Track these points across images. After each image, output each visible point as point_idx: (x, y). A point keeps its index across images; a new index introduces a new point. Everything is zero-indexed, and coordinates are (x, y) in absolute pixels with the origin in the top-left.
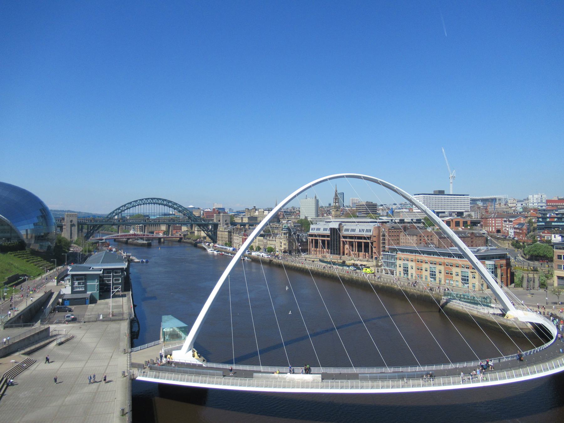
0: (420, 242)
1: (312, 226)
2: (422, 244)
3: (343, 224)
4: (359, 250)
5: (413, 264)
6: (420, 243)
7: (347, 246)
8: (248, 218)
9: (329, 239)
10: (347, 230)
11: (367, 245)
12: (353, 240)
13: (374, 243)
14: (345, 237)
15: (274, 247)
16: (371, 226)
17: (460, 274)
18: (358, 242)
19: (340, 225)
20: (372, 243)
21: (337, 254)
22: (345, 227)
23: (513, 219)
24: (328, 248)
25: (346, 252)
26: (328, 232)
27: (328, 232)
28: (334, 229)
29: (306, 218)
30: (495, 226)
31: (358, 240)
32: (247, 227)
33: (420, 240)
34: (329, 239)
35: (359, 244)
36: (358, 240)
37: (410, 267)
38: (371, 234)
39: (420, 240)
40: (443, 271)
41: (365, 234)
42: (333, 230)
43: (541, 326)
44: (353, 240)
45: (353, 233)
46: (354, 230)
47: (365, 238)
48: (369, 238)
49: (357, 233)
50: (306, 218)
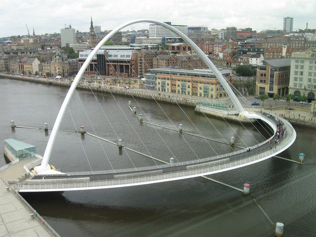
0: (168, 64)
1: (81, 53)
2: (170, 66)
3: (107, 51)
4: (122, 71)
5: (169, 82)
6: (169, 65)
7: (112, 68)
8: (16, 46)
9: (96, 63)
10: (110, 56)
11: (127, 67)
12: (116, 64)
13: (133, 66)
14: (108, 62)
15: (49, 72)
16: (130, 53)
17: (203, 88)
18: (120, 65)
19: (105, 51)
20: (131, 65)
21: (103, 75)
22: (109, 54)
23: (221, 46)
24: (96, 70)
25: (111, 73)
26: (96, 58)
27: (96, 58)
28: (100, 55)
29: (68, 45)
30: (209, 50)
31: (120, 64)
32: (19, 54)
33: (169, 63)
34: (96, 63)
35: (121, 67)
36: (120, 64)
37: (166, 84)
38: (130, 58)
39: (169, 63)
40: (191, 87)
41: (125, 58)
42: (99, 56)
43: (259, 120)
44: (116, 64)
45: (115, 58)
46: (116, 56)
47: (125, 62)
48: (129, 62)
49: (119, 58)
50: (68, 45)
